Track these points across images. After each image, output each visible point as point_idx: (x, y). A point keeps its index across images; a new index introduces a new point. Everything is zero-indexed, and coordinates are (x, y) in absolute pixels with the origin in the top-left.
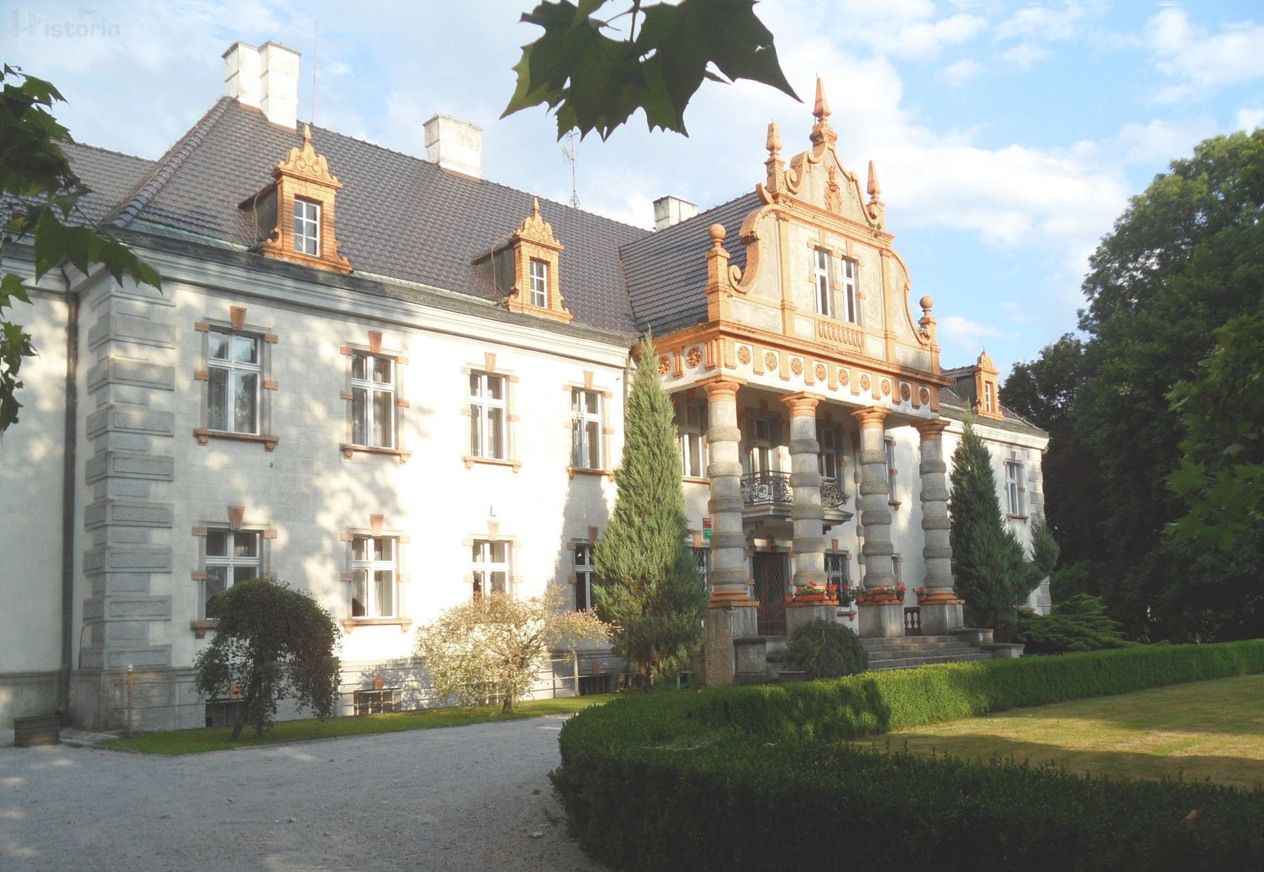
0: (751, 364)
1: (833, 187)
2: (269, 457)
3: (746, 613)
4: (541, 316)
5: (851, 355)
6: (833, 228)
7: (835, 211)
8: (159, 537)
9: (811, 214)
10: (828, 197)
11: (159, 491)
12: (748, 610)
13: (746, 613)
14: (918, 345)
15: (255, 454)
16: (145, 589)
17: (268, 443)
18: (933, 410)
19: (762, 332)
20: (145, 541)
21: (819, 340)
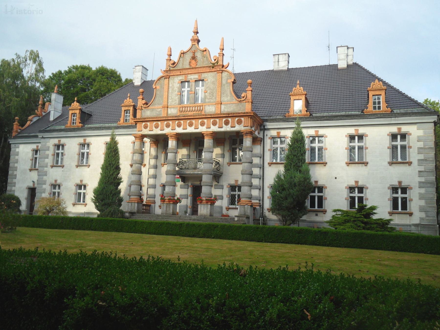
0: (148, 128)
1: (194, 58)
2: (63, 169)
3: (132, 204)
4: (126, 125)
5: (199, 115)
6: (190, 73)
7: (193, 66)
8: (44, 186)
9: (179, 72)
10: (190, 62)
11: (45, 178)
12: (133, 204)
13: (132, 204)
14: (237, 102)
15: (60, 169)
16: (41, 196)
17: (63, 167)
18: (244, 126)
19: (148, 118)
20: (42, 187)
21: (178, 114)
